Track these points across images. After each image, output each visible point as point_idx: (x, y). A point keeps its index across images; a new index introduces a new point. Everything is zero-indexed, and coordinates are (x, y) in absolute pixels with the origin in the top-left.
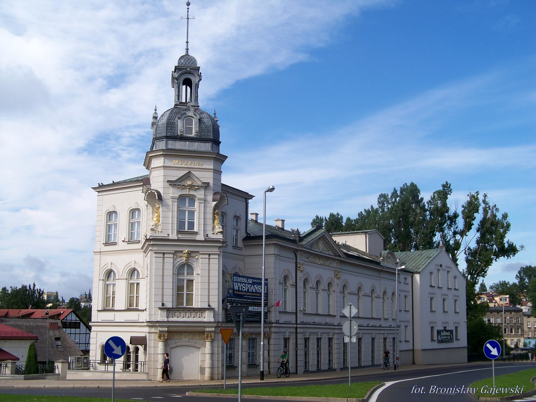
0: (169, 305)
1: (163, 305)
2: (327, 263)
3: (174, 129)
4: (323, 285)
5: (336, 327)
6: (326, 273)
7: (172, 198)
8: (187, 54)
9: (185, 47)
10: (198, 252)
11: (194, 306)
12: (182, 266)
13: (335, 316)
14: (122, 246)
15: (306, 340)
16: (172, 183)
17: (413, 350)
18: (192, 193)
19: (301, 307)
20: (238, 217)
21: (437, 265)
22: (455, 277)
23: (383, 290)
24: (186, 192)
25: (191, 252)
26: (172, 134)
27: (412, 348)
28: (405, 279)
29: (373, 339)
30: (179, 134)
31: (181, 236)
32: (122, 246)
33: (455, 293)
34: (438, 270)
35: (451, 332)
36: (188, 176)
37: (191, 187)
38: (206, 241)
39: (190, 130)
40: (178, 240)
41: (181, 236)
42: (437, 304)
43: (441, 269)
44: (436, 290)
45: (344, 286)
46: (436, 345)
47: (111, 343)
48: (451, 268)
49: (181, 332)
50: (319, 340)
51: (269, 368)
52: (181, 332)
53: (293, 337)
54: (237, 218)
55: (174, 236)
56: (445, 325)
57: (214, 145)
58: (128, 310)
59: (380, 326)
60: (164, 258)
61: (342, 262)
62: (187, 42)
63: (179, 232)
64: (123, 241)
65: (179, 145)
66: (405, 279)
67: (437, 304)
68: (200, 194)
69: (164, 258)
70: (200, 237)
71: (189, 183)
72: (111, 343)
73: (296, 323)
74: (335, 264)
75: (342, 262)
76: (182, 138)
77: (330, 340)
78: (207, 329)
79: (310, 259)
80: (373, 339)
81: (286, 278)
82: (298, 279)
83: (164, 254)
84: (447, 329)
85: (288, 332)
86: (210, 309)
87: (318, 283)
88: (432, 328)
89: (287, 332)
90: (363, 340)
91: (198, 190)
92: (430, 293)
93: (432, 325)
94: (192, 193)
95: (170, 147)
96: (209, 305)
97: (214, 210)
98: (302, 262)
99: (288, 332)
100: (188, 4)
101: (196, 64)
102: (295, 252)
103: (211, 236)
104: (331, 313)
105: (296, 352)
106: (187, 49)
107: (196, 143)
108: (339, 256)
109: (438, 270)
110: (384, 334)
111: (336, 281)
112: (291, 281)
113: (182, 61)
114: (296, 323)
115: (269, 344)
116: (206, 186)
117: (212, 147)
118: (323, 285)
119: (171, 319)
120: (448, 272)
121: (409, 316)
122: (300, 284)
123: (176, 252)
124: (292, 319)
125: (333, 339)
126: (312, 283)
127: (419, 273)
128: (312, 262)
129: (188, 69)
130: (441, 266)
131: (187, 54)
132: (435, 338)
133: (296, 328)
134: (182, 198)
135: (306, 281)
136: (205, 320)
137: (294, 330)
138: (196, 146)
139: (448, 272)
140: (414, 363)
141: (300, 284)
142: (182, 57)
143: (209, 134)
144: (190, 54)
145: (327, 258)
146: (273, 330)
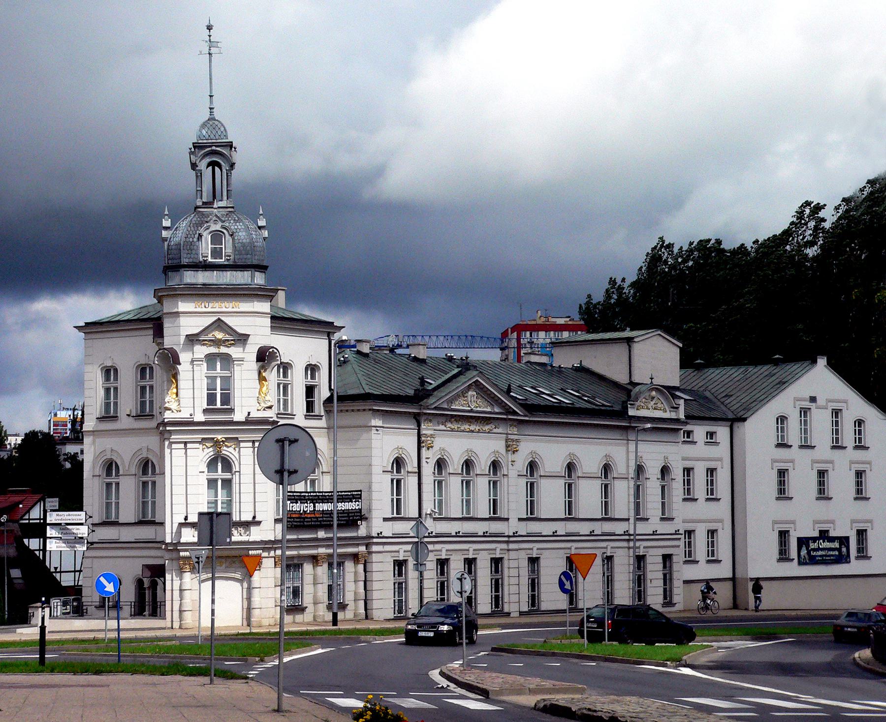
1: (186, 518)
2: (486, 428)
3: (194, 252)
4: (482, 465)
5: (511, 539)
6: (485, 446)
8: (212, 119)
9: (208, 105)
13: (507, 519)
14: (125, 422)
15: (443, 564)
16: (193, 340)
18: (223, 350)
19: (428, 507)
20: (315, 365)
21: (797, 399)
22: (860, 423)
23: (632, 464)
24: (213, 350)
26: (191, 260)
27: (730, 575)
28: (711, 434)
29: (534, 561)
30: (201, 259)
32: (125, 422)
33: (860, 455)
34: (804, 412)
35: (844, 541)
36: (219, 324)
42: (802, 482)
43: (813, 406)
44: (795, 453)
45: (532, 466)
46: (793, 569)
47: (102, 579)
48: (845, 402)
50: (470, 563)
51: (366, 609)
54: (312, 369)
55: (200, 417)
56: (824, 527)
57: (257, 274)
58: (140, 523)
60: (186, 448)
64: (128, 415)
66: (711, 434)
67: (802, 482)
68: (235, 352)
69: (186, 448)
72: (102, 579)
76: (207, 267)
77: (496, 563)
79: (449, 425)
80: (534, 561)
81: (399, 463)
82: (424, 460)
83: (185, 443)
84: (832, 534)
85: (403, 551)
87: (468, 465)
88: (783, 535)
89: (402, 552)
90: (543, 562)
91: (232, 348)
92: (774, 461)
93: (784, 527)
94: (223, 350)
96: (254, 517)
97: (260, 373)
98: (429, 432)
99: (403, 551)
100: (209, 28)
103: (255, 414)
105: (421, 582)
107: (229, 273)
109: (804, 412)
110: (570, 548)
111: (511, 457)
112: (411, 464)
113: (204, 132)
115: (365, 571)
117: (253, 277)
118: (482, 465)
120: (836, 413)
121: (722, 509)
122: (428, 469)
123: (203, 439)
125: (478, 561)
126: (455, 464)
128: (452, 430)
130: (813, 399)
131: (212, 119)
132: (794, 553)
134: (211, 359)
135: (440, 464)
136: (251, 539)
139: (836, 413)
141: (428, 469)
142: (204, 125)
145: (486, 420)
146: (375, 548)
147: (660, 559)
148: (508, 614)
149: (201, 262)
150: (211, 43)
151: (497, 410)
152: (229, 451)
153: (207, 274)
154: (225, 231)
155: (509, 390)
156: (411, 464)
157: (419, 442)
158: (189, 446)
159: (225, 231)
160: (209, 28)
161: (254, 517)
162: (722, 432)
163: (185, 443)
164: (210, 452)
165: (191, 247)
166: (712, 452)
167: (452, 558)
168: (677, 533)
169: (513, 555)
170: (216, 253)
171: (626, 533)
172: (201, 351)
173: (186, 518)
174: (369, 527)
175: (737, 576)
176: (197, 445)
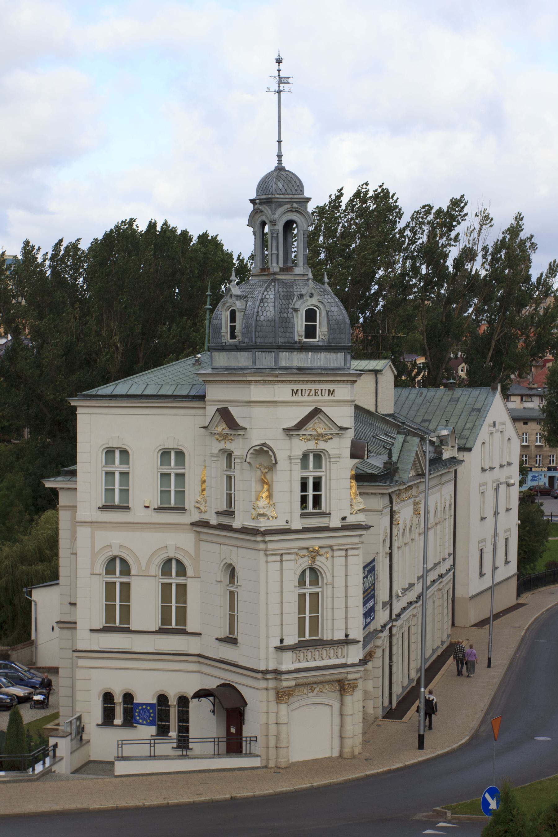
3: (289, 330)
10: (330, 547)
11: (327, 636)
18: (322, 445)
26: (286, 340)
30: (297, 339)
32: (138, 513)
38: (344, 528)
39: (310, 332)
55: (297, 524)
62: (279, 142)
65: (297, 359)
70: (335, 523)
71: (320, 431)
76: (303, 348)
94: (322, 445)
95: (283, 364)
100: (279, 61)
101: (302, 191)
103: (352, 519)
106: (280, 156)
129: (295, 205)
131: (280, 169)
138: (323, 359)
143: (342, 336)
144: (287, 164)
149: (296, 342)
150: (281, 80)
152: (321, 563)
153: (302, 355)
154: (321, 306)
158: (285, 557)
159: (321, 306)
161: (347, 635)
163: (282, 554)
164: (305, 563)
165: (285, 323)
170: (310, 332)
172: (300, 446)
173: (282, 641)
176: (293, 557)
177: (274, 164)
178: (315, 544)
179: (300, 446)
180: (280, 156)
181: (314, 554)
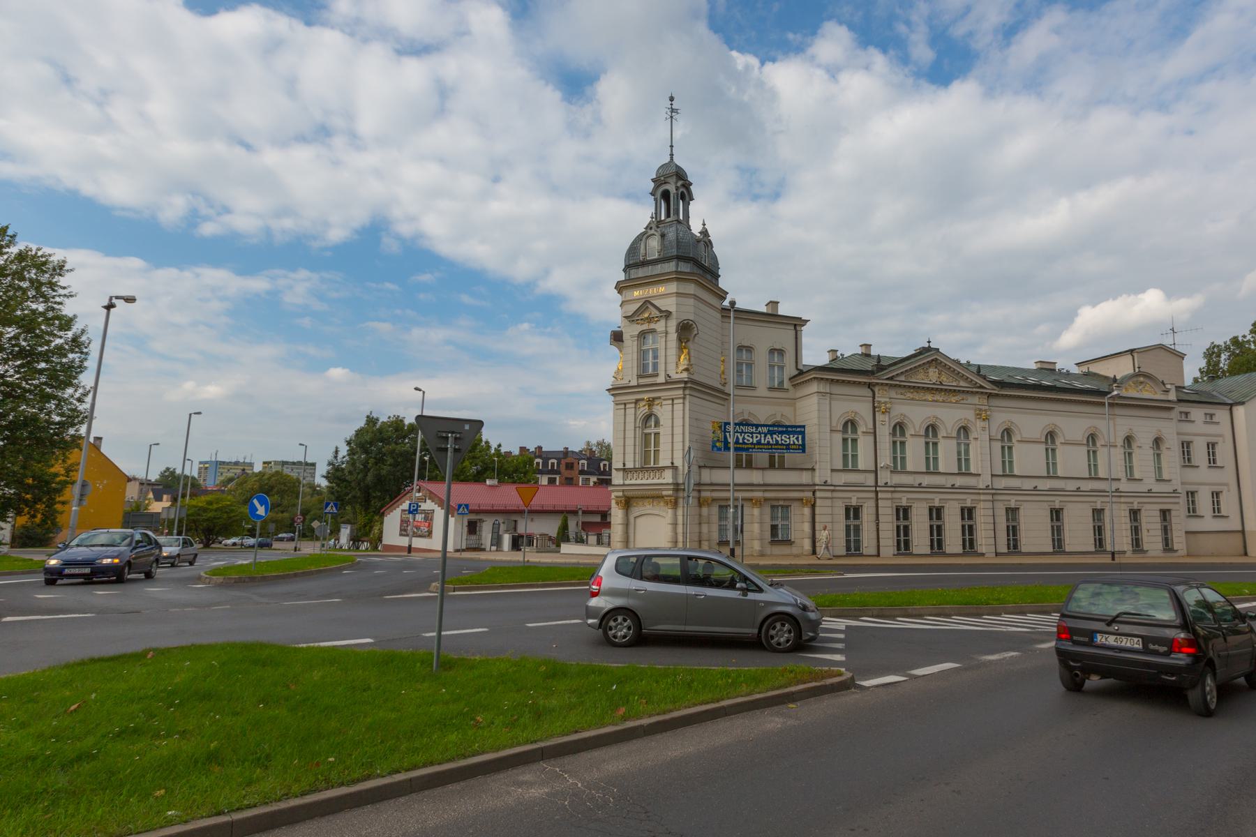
0: (630, 465)
2: (953, 399)
7: (632, 337)
12: (648, 418)
17: (1243, 532)
18: (652, 326)
24: (645, 327)
25: (654, 399)
27: (1240, 528)
31: (643, 381)
37: (650, 320)
38: (667, 383)
40: (638, 386)
41: (643, 381)
49: (643, 498)
50: (936, 513)
52: (643, 498)
53: (872, 503)
55: (634, 383)
59: (1117, 490)
61: (990, 395)
63: (639, 377)
68: (660, 326)
71: (646, 315)
73: (876, 486)
74: (975, 400)
75: (990, 395)
78: (665, 493)
86: (673, 467)
94: (652, 326)
98: (883, 400)
102: (870, 386)
103: (675, 376)
104: (973, 470)
105: (878, 525)
106: (672, 155)
108: (981, 387)
111: (980, 424)
114: (876, 486)
116: (667, 315)
117: (677, 266)
119: (627, 482)
124: (870, 479)
127: (1242, 403)
133: (877, 492)
137: (873, 495)
138: (659, 269)
140: (1246, 554)
147: (1158, 513)
148: (983, 554)
150: (673, 110)
151: (962, 384)
152: (657, 410)
153: (645, 269)
155: (979, 371)
156: (864, 425)
157: (874, 408)
160: (672, 99)
162: (1221, 415)
164: (643, 409)
166: (1211, 429)
167: (947, 506)
168: (1175, 491)
169: (982, 505)
171: (1117, 490)
172: (638, 328)
174: (813, 477)
175: (1247, 529)
177: (667, 160)
178: (646, 396)
179: (638, 328)
180: (672, 155)
181: (651, 402)
